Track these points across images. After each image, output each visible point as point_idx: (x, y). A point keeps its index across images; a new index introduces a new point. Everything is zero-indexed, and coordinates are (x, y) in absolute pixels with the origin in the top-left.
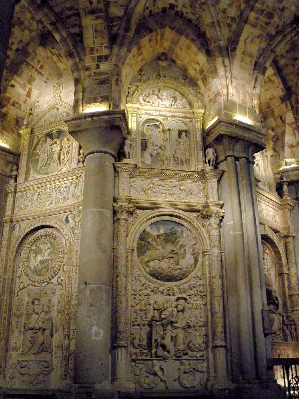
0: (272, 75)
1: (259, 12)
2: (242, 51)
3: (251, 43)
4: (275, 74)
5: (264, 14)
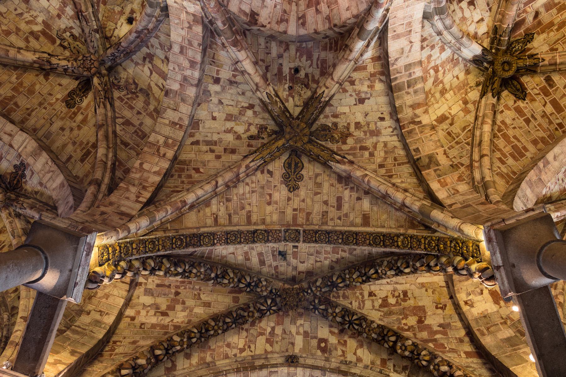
0: (287, 28)
1: (413, 82)
2: (412, 33)
3: (403, 49)
4: (285, 32)
5: (406, 84)
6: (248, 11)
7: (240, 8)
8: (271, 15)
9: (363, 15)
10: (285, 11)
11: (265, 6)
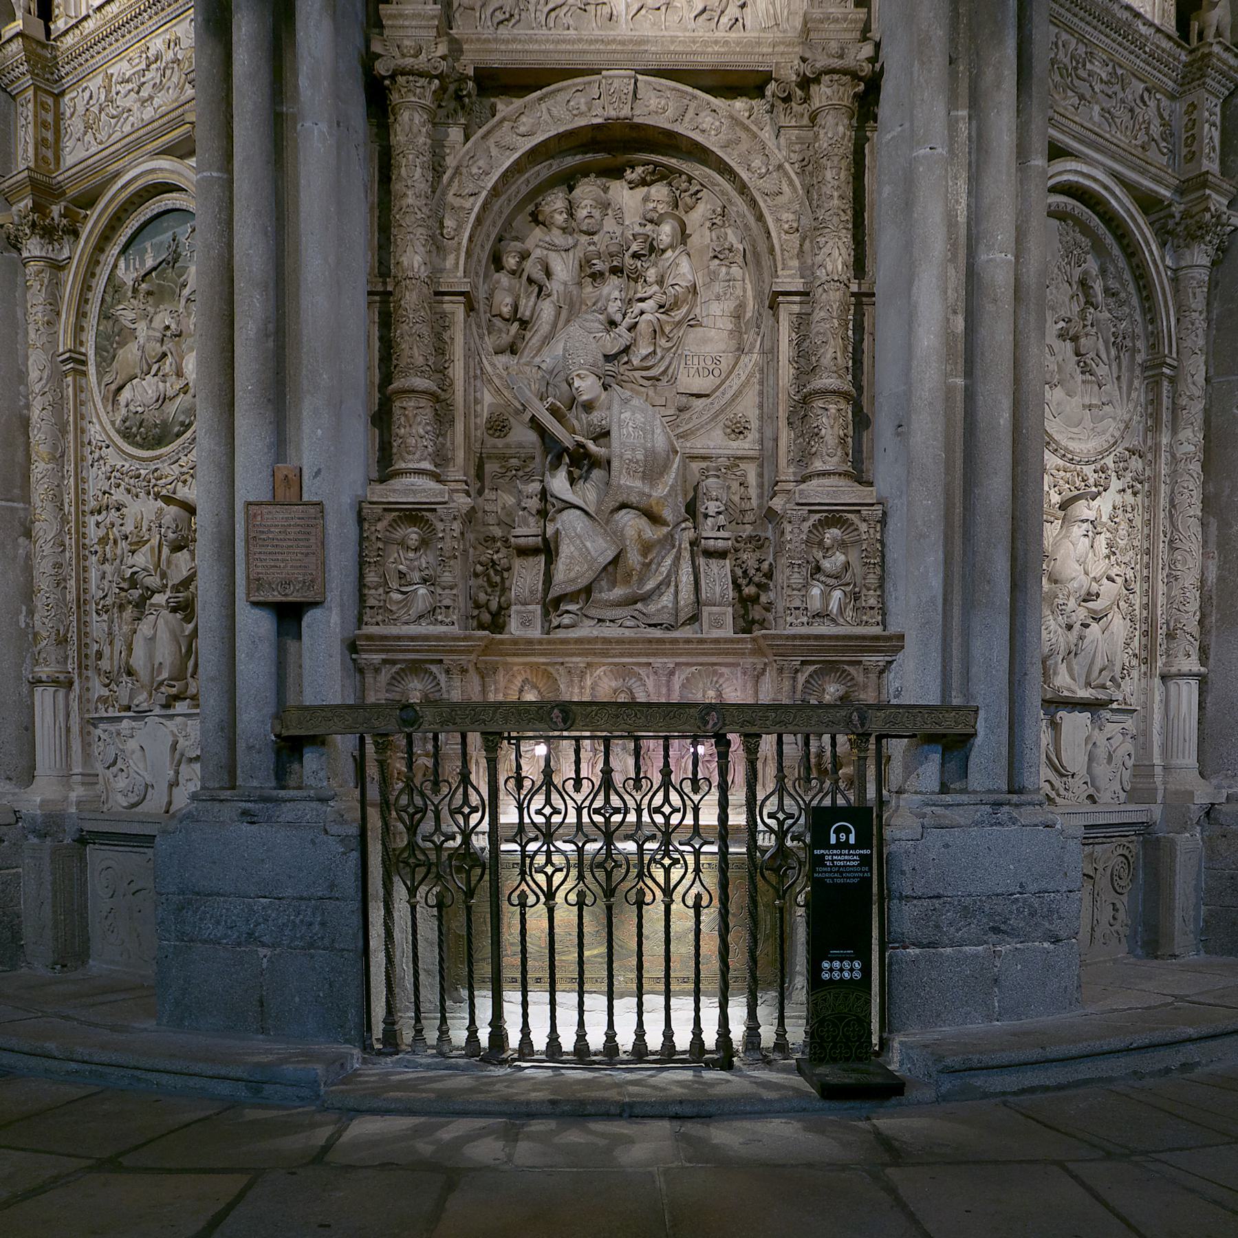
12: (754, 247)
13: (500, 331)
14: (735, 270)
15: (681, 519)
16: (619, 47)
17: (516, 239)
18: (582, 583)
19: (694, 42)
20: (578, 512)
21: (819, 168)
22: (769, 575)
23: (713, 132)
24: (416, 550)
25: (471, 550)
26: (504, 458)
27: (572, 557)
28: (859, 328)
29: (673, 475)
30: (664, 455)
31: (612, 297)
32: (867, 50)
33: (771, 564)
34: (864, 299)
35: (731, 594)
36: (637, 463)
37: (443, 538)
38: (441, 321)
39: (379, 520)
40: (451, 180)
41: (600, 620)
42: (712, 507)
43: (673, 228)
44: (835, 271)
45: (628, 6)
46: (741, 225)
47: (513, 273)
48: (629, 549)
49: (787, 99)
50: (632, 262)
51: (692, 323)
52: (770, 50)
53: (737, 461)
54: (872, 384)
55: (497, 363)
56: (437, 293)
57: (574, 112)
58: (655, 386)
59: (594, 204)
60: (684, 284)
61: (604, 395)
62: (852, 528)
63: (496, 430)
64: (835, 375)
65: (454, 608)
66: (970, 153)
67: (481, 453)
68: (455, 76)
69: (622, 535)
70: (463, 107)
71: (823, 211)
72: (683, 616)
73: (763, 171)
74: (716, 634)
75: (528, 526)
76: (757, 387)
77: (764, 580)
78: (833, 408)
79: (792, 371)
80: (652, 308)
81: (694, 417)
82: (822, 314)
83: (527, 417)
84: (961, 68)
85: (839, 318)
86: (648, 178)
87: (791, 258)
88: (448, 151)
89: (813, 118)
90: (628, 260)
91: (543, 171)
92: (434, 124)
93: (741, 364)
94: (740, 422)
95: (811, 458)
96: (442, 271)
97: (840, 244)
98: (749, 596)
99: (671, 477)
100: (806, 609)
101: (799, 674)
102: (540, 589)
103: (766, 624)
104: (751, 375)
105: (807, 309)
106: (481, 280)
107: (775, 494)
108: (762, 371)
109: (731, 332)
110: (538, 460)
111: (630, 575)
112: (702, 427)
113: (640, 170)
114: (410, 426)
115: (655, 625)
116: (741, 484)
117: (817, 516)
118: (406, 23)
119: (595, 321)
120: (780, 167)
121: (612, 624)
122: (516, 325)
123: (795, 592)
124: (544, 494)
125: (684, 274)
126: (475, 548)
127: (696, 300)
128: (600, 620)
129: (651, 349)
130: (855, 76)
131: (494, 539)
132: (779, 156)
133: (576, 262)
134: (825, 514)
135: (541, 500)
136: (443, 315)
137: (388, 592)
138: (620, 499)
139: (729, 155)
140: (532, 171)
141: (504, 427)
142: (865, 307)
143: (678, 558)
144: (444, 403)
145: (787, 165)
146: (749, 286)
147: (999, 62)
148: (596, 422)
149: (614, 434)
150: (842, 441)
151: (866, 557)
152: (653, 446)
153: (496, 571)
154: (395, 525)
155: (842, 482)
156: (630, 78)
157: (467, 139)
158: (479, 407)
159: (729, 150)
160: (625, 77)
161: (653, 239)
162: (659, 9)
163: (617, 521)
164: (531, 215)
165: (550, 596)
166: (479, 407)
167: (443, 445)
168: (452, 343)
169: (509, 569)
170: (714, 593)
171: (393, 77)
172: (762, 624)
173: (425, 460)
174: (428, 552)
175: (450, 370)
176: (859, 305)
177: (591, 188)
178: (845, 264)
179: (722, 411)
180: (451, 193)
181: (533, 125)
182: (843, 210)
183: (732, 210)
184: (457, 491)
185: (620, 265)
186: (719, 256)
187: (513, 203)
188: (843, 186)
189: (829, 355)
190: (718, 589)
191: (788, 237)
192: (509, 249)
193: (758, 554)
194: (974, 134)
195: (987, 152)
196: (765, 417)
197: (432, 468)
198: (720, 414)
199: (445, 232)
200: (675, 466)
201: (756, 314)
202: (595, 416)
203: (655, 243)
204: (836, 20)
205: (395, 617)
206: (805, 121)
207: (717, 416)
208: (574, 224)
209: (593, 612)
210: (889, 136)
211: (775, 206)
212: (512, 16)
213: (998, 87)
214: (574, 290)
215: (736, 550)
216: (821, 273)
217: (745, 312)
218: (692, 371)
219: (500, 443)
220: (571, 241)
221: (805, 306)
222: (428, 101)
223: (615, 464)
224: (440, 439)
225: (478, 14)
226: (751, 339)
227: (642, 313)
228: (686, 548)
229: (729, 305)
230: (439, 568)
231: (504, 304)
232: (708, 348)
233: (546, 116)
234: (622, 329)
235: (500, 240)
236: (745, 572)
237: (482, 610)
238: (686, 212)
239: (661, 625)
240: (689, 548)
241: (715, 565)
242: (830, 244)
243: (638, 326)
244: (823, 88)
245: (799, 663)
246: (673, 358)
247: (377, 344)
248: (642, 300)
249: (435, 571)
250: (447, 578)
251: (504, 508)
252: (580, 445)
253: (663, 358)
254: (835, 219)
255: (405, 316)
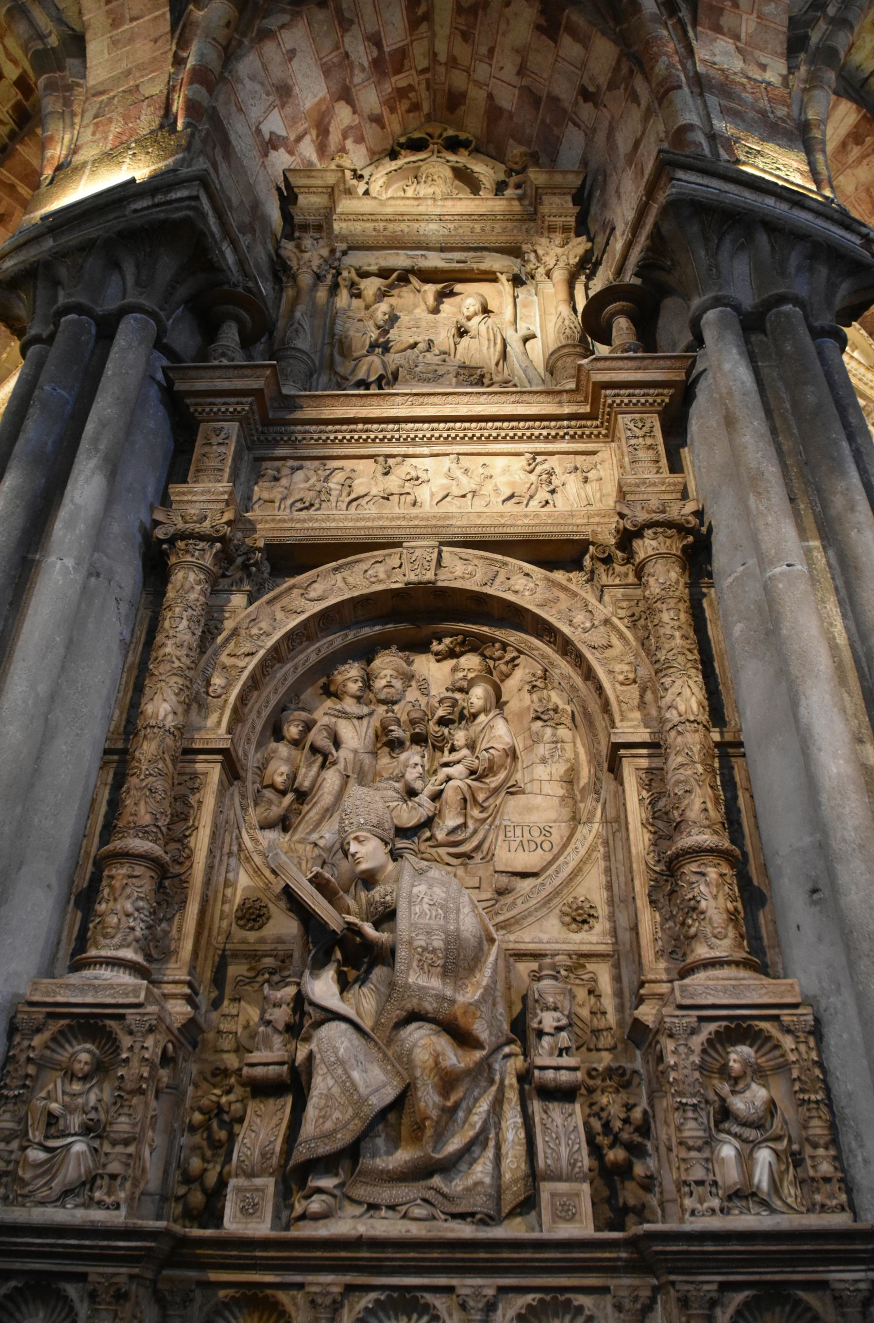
6: (566, 40)
7: (586, 47)
8: (503, 26)
9: (246, 42)
10: (466, 36)
11: (517, 51)
12: (585, 708)
13: (270, 802)
14: (563, 732)
15: (502, 1040)
16: (422, 523)
17: (303, 709)
18: (343, 1139)
19: (502, 516)
20: (343, 1026)
21: (651, 611)
22: (644, 1129)
23: (527, 593)
24: (85, 1078)
25: (190, 1089)
26: (253, 956)
27: (329, 1097)
28: (729, 784)
29: (488, 972)
30: (473, 942)
31: (412, 762)
32: (690, 507)
33: (645, 1112)
34: (731, 750)
35: (585, 1161)
36: (434, 951)
37: (127, 1061)
38: (190, 784)
39: (38, 1030)
40: (227, 640)
41: (373, 1207)
42: (549, 1020)
43: (486, 690)
44: (689, 711)
45: (432, 495)
46: (567, 687)
47: (296, 743)
48: (419, 1083)
49: (608, 561)
50: (437, 729)
51: (514, 790)
52: (585, 521)
53: (582, 961)
54: (760, 848)
55: (260, 838)
56: (187, 751)
57: (373, 579)
58: (464, 865)
59: (395, 673)
60: (500, 746)
61: (391, 866)
62: (768, 1046)
63: (248, 920)
64: (708, 831)
65: (125, 1179)
66: (833, 578)
67: (224, 950)
68: (243, 549)
69: (410, 1061)
70: (249, 575)
71: (664, 652)
72: (509, 1200)
73: (588, 625)
74: (566, 1231)
75: (271, 1049)
76: (602, 864)
77: (637, 1139)
78: (712, 873)
79: (647, 836)
80: (461, 774)
81: (519, 901)
82: (680, 759)
83: (278, 888)
84: (802, 506)
85: (702, 763)
86: (457, 649)
87: (632, 710)
88: (227, 615)
89: (639, 572)
90: (433, 727)
91: (337, 640)
92: (214, 592)
93: (578, 835)
94: (581, 908)
95: (689, 945)
96: (199, 729)
97: (691, 682)
98: (615, 1164)
99: (484, 976)
100: (715, 1183)
101: (718, 1311)
102: (278, 1149)
103: (647, 1214)
104: (592, 849)
105: (657, 763)
106: (253, 747)
107: (641, 1000)
108: (606, 843)
109: (563, 798)
110: (296, 955)
111: (419, 1127)
112: (530, 914)
113: (447, 641)
114: (115, 900)
115: (462, 1216)
116: (590, 992)
117: (712, 1027)
118: (195, 498)
119: (390, 791)
120: (607, 622)
121: (390, 1213)
122: (290, 797)
123: (693, 1154)
124: (300, 1001)
125: (500, 736)
126: (196, 1086)
127: (516, 766)
128: (373, 1207)
129: (460, 821)
130: (680, 528)
131: (225, 1073)
132: (603, 610)
133: (371, 732)
134: (724, 1023)
135: (294, 1011)
136: (194, 776)
137: (26, 1148)
138: (409, 1006)
139: (547, 612)
140: (325, 640)
141: (260, 916)
142: (733, 760)
143: (498, 1103)
144: (176, 880)
145: (615, 620)
146: (581, 750)
147: (847, 489)
148: (377, 898)
149: (402, 913)
150: (732, 916)
151: (802, 1091)
152: (458, 929)
153: (222, 1124)
154: (63, 1041)
155: (743, 973)
156: (433, 548)
157: (250, 602)
158: (229, 892)
159: (546, 608)
160: (428, 547)
161: (464, 708)
162: (464, 496)
163: (403, 1041)
164: (321, 688)
165: (291, 1163)
166: (229, 892)
167: (166, 933)
168: (199, 808)
169: (241, 1120)
170: (559, 1159)
171: (172, 541)
172: (641, 1212)
173: (128, 946)
174: (107, 1087)
175: (192, 839)
176: (725, 758)
177: (392, 659)
178: (700, 704)
179: (557, 893)
180: (226, 653)
181: (325, 591)
182: (690, 650)
183: (555, 673)
184: (174, 996)
185: (424, 732)
186: (543, 716)
187: (300, 671)
188: (684, 626)
189: (697, 806)
190: (564, 1152)
191: (624, 688)
192: (291, 718)
193: (623, 1096)
194: (834, 561)
195: (856, 568)
196: (616, 899)
197: (139, 958)
198: (555, 897)
199: (211, 689)
200: (491, 959)
201: (593, 779)
202: (377, 893)
203: (466, 712)
204: (654, 484)
205: (26, 1191)
206: (631, 579)
207: (550, 900)
208: (371, 696)
209: (361, 1192)
210: (730, 580)
211: (605, 658)
212: (312, 505)
213: (853, 509)
214: (367, 759)
215: (591, 1091)
216: (672, 716)
217: (579, 779)
218: (514, 845)
219: (252, 936)
220: (365, 710)
221: (656, 760)
222: (208, 561)
223: (402, 953)
224: (164, 925)
225: (277, 504)
226: (589, 807)
227: (449, 779)
228: (511, 1086)
229: (560, 769)
230: (114, 1109)
231: (279, 772)
232: (533, 818)
233: (340, 584)
234: (423, 798)
235: (284, 709)
236: (606, 1125)
237: (193, 1186)
238: (502, 681)
239: (472, 1215)
240: (516, 1085)
241: (558, 1111)
242: (679, 682)
243: (444, 795)
244: (647, 541)
245: (715, 1287)
246: (489, 830)
247: (103, 809)
248: (446, 765)
249: (107, 1112)
250: (123, 1125)
251: (246, 1027)
252: (352, 929)
253: (475, 832)
254: (681, 659)
255: (136, 767)
